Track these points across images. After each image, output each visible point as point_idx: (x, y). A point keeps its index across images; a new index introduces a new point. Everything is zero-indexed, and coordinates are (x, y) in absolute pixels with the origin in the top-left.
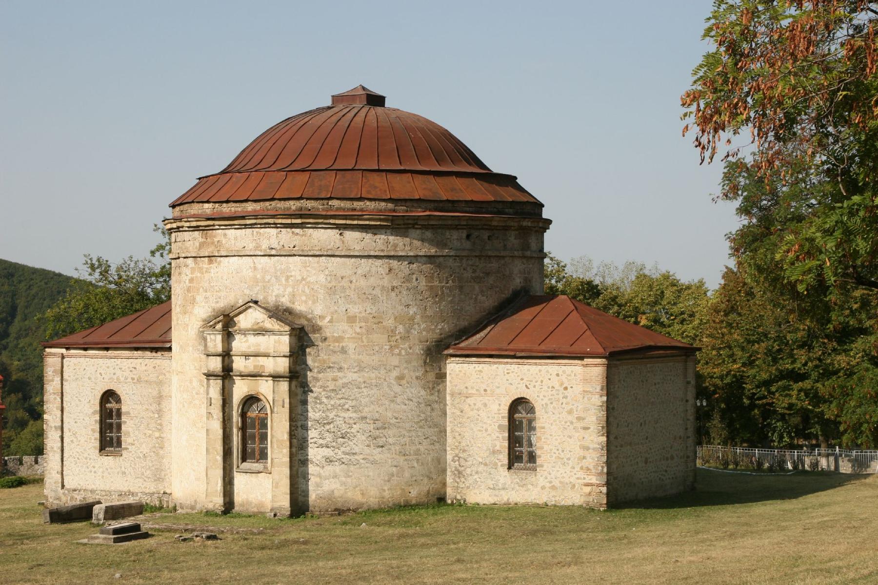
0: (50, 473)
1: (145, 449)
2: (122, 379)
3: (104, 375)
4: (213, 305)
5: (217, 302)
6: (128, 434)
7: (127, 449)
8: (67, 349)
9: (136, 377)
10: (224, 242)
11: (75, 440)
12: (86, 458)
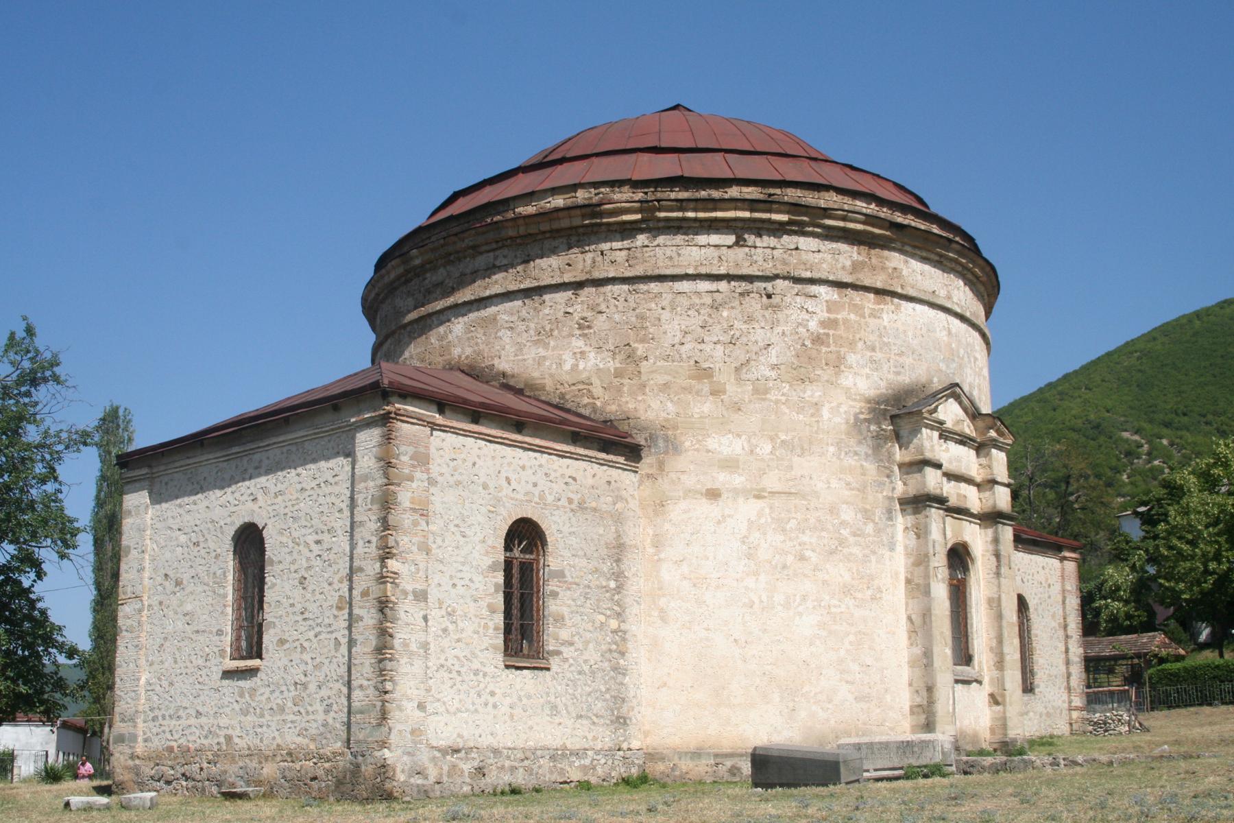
0: (400, 708)
1: (592, 655)
2: (550, 499)
3: (514, 485)
4: (891, 376)
5: (898, 373)
6: (560, 619)
7: (558, 653)
8: (441, 411)
9: (576, 497)
10: (905, 272)
11: (451, 627)
12: (476, 673)
